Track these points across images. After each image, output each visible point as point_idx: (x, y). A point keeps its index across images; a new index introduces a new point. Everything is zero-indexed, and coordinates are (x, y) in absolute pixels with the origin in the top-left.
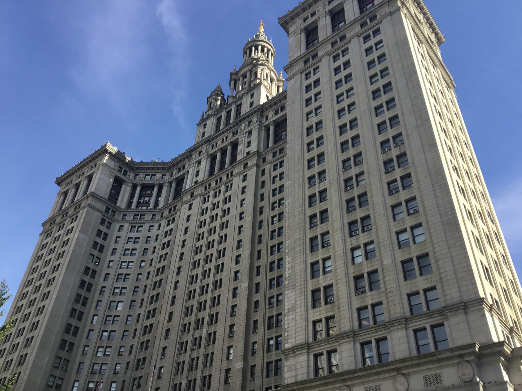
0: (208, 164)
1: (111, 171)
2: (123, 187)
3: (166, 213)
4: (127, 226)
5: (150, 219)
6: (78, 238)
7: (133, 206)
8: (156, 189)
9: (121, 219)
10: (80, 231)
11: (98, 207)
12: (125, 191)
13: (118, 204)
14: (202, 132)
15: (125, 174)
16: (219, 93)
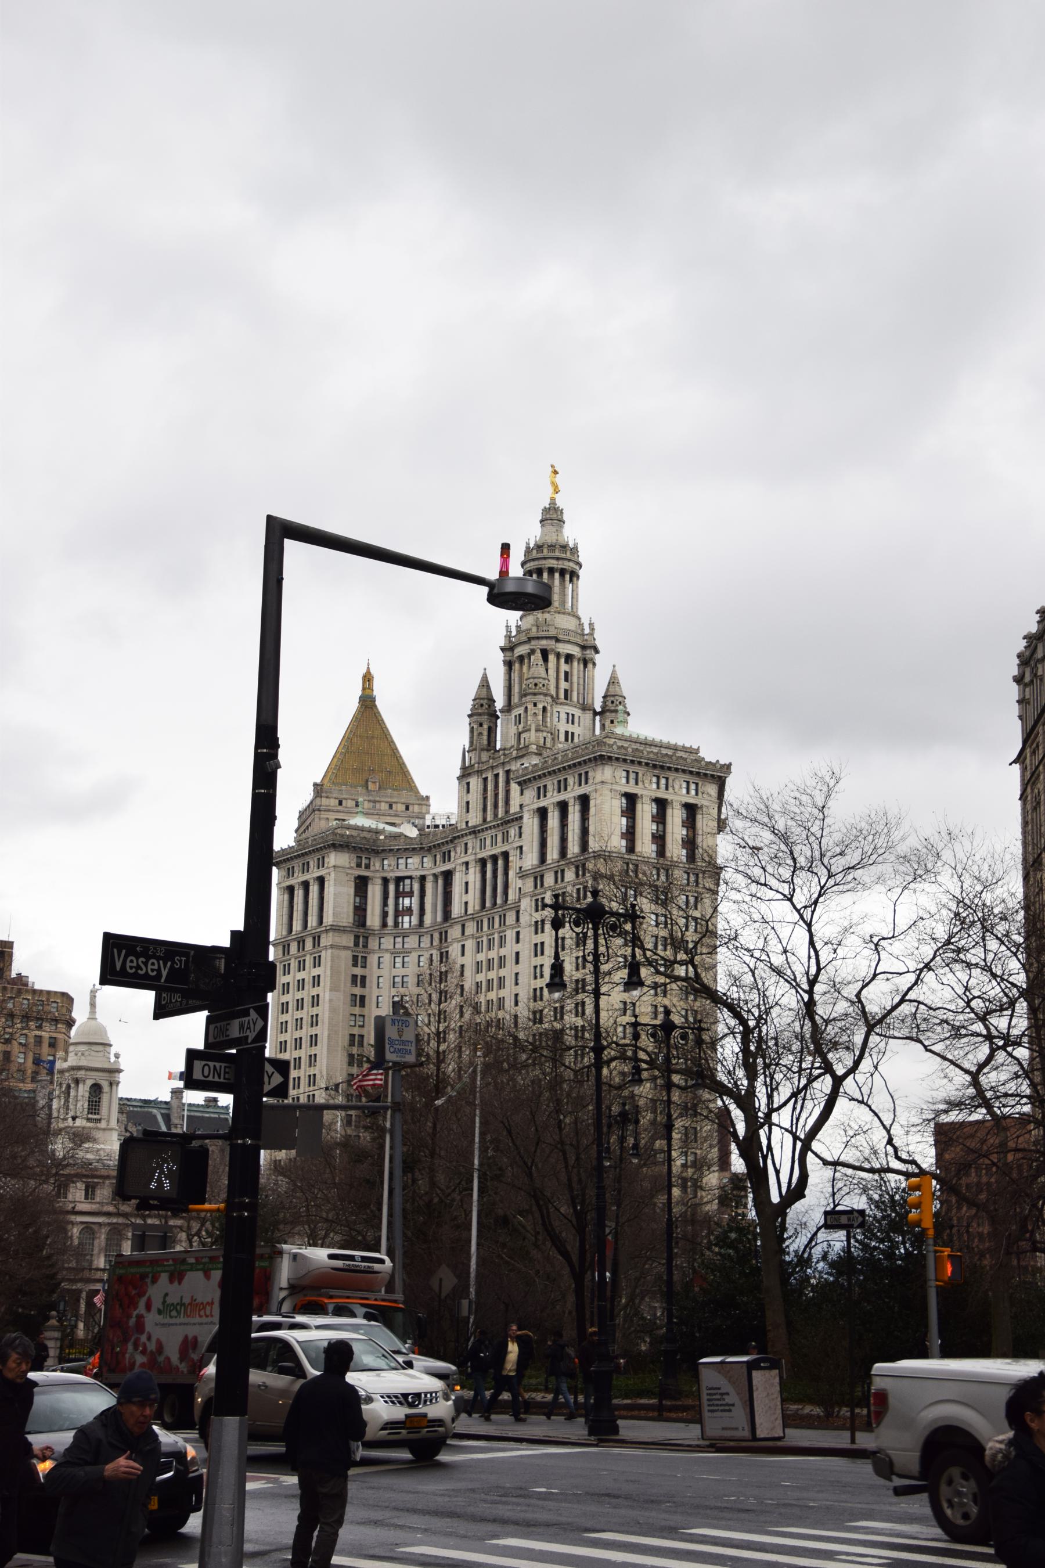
0: (478, 876)
1: (347, 874)
2: (370, 888)
3: (436, 936)
4: (387, 958)
5: (417, 946)
6: (331, 1000)
7: (390, 921)
8: (416, 887)
9: (377, 948)
10: (331, 990)
11: (344, 943)
12: (374, 891)
13: (368, 923)
14: (465, 800)
15: (368, 867)
16: (484, 702)
